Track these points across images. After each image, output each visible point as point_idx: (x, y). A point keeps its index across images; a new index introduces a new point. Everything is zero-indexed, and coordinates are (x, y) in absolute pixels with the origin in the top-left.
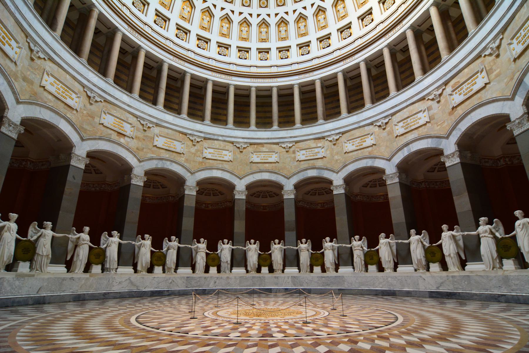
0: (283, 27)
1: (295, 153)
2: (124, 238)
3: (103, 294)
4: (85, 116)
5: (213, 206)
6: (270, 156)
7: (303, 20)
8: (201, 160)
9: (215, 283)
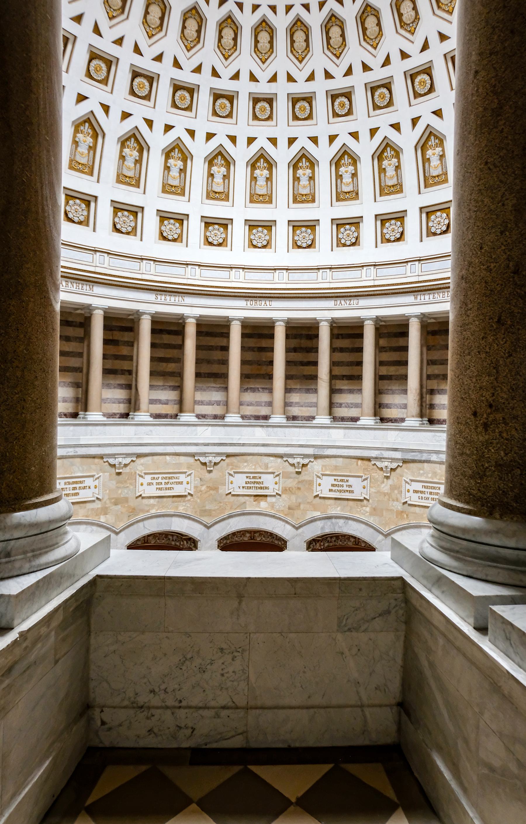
4: (206, 493)
8: (400, 507)
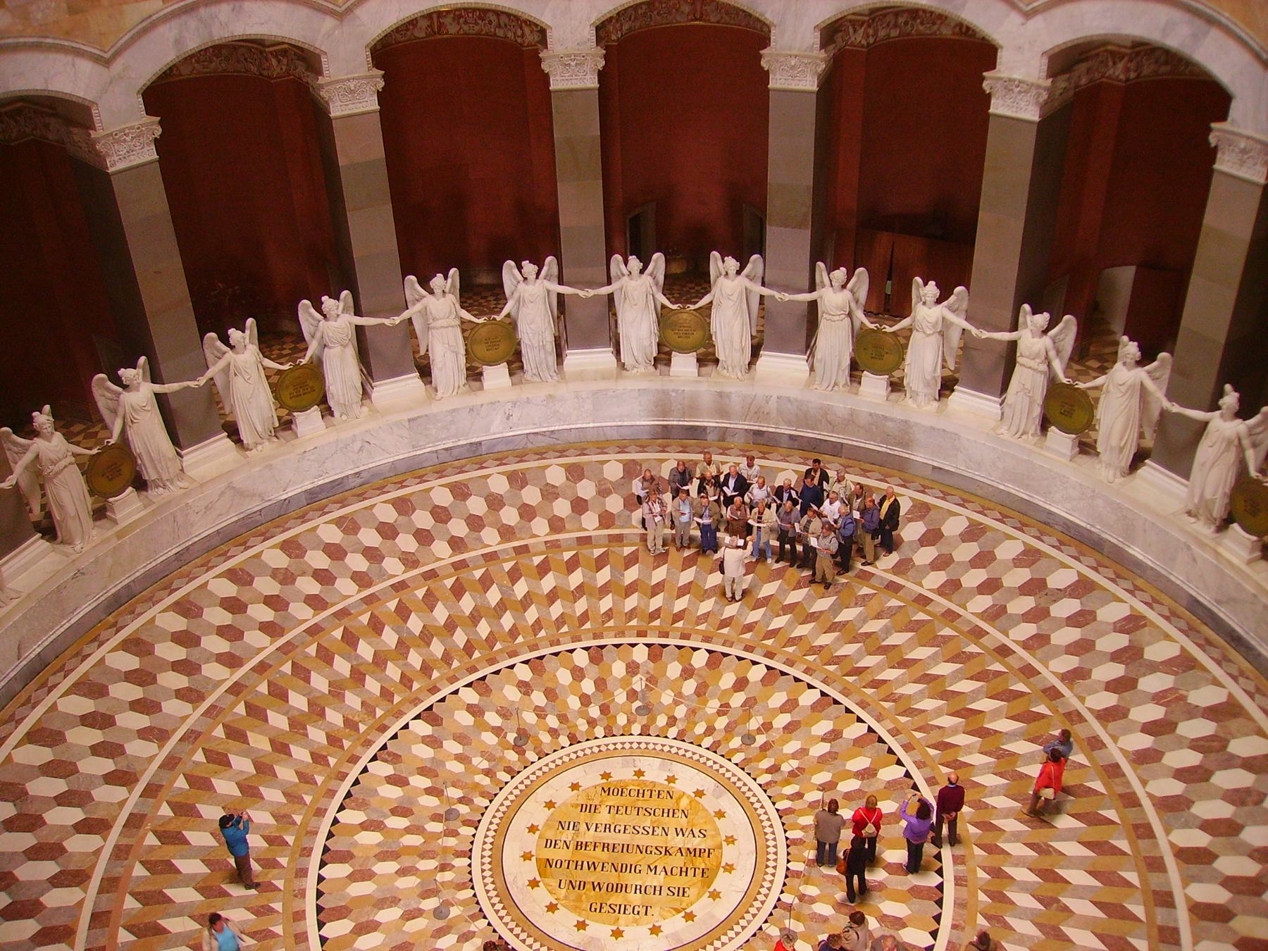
2: (165, 368)
3: (174, 558)
5: (466, 23)
9: (508, 419)
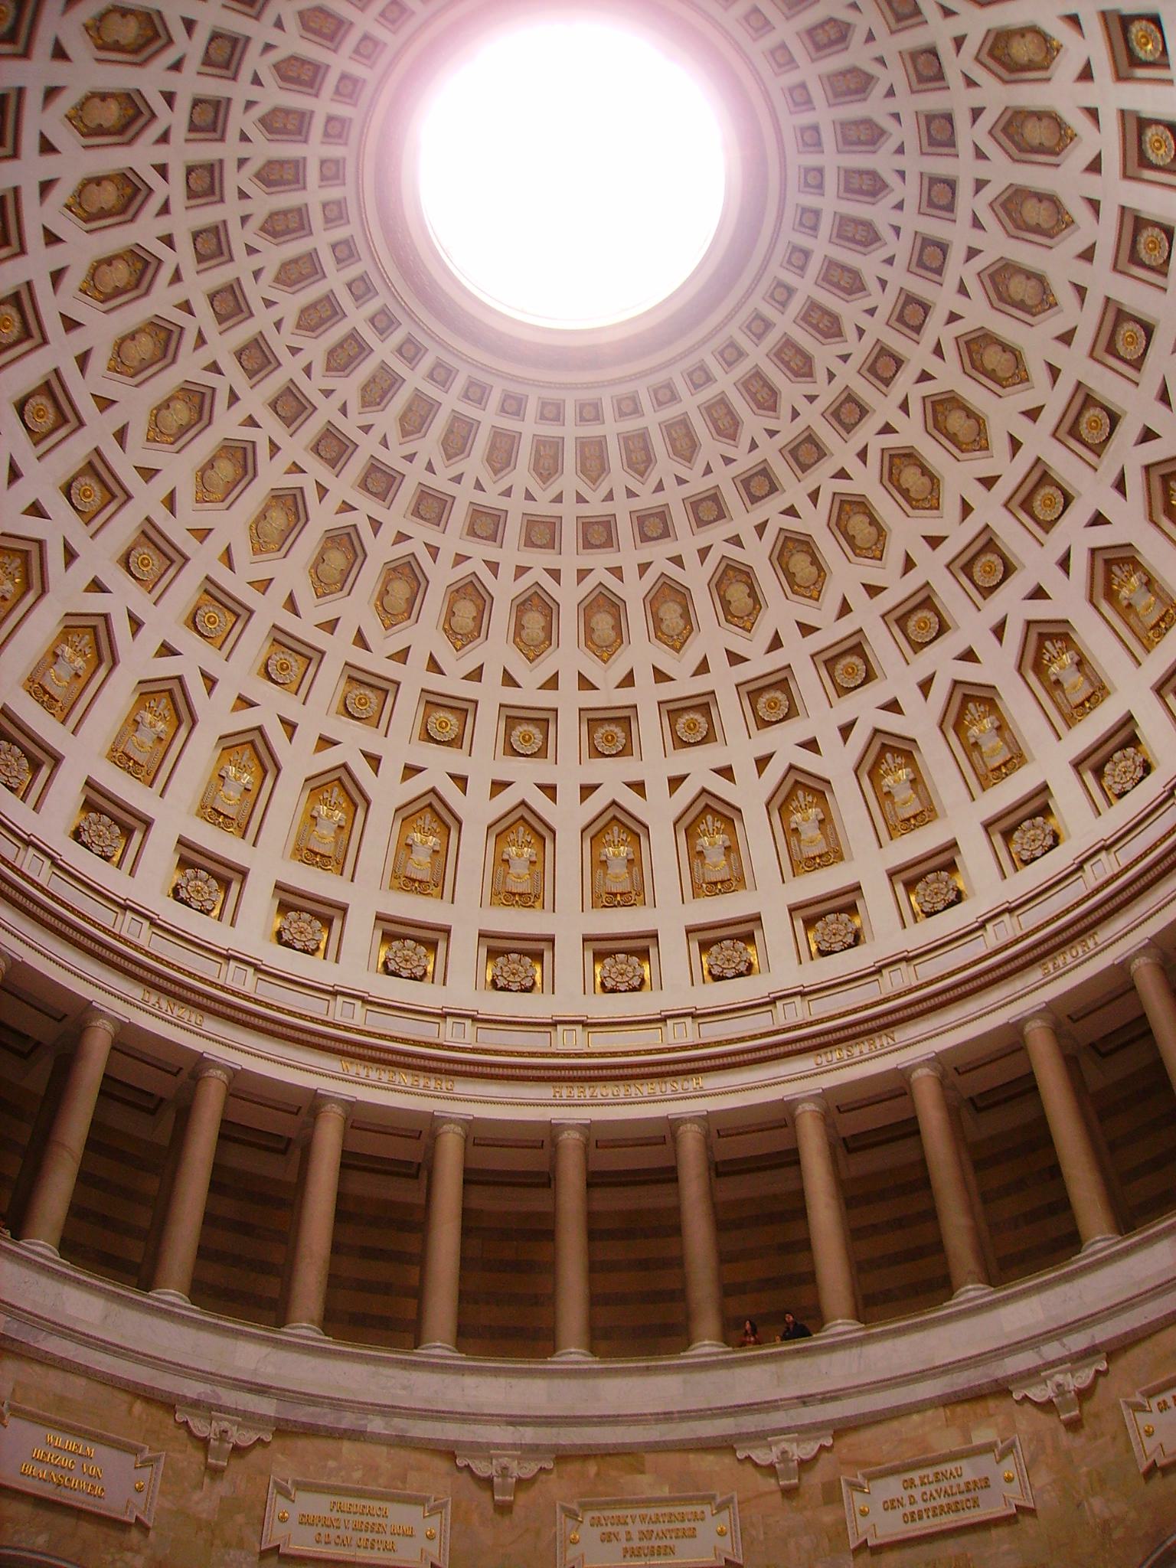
0: (711, 835)
1: (841, 1500)
6: (686, 1525)
7: (810, 799)
